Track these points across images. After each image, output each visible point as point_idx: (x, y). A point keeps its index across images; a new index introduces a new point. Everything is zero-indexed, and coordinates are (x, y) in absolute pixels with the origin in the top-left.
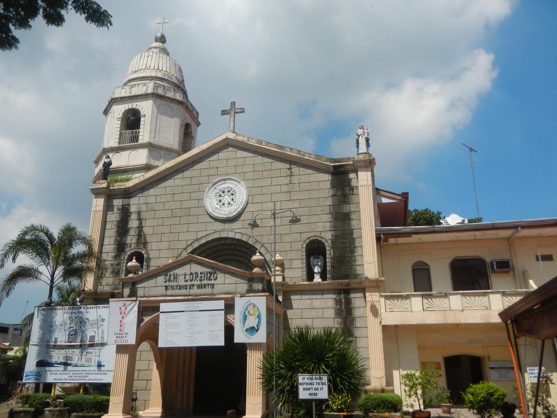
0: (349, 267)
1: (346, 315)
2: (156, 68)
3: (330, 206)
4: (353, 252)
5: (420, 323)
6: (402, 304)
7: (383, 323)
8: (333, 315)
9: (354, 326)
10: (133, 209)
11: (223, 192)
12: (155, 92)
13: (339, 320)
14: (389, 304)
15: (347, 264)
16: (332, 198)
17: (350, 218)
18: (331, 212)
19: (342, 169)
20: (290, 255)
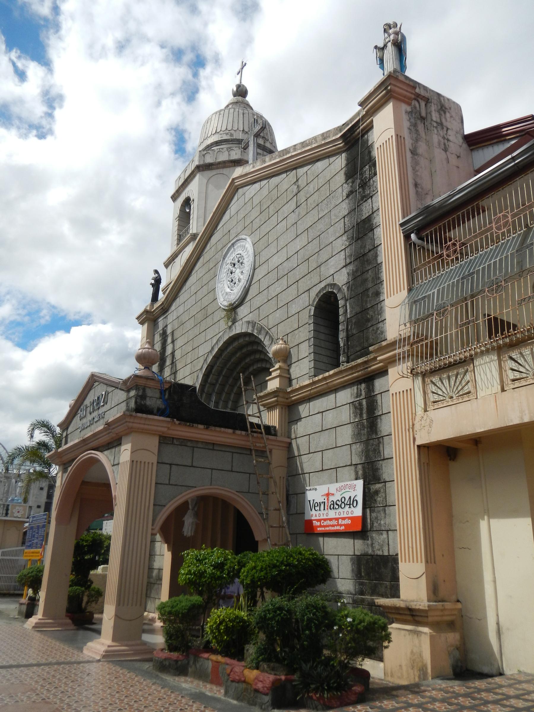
0: (373, 330)
1: (369, 434)
3: (344, 217)
4: (378, 294)
5: (492, 428)
6: (452, 383)
7: (419, 442)
8: (350, 436)
9: (380, 455)
10: (169, 331)
11: (234, 265)
12: (202, 163)
13: (358, 448)
14: (433, 393)
15: (370, 325)
16: (347, 201)
17: (373, 224)
18: (346, 230)
19: (356, 133)
20: (297, 336)
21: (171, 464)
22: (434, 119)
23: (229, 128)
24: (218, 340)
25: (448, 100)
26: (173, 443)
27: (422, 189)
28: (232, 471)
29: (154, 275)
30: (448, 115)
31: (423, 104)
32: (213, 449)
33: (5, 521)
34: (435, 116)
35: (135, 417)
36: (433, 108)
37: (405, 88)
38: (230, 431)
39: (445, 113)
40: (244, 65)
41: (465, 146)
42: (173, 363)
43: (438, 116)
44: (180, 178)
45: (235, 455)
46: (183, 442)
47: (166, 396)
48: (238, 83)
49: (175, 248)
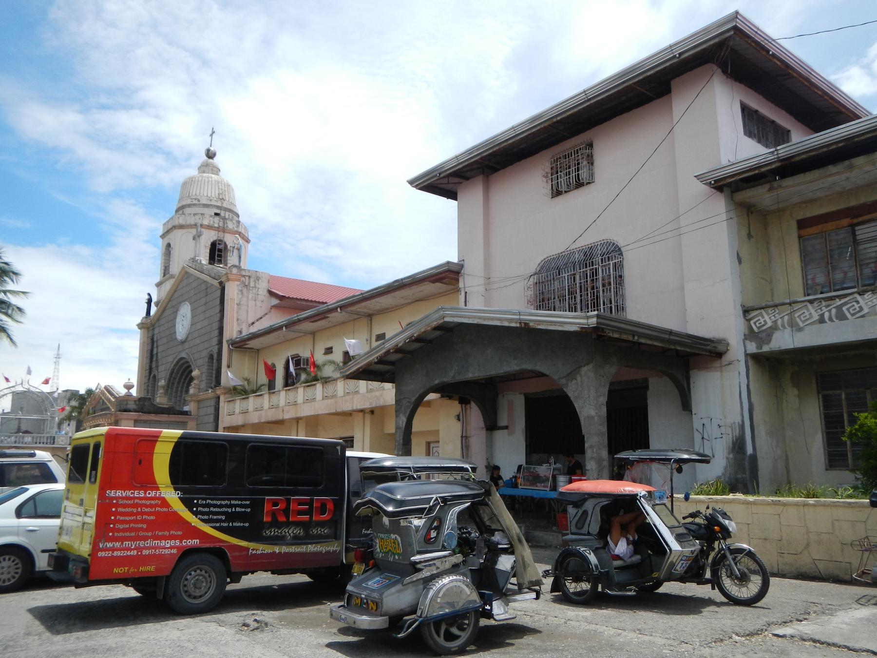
2: (187, 195)
10: (155, 339)
22: (251, 286)
23: (198, 193)
24: (176, 356)
29: (147, 297)
30: (260, 281)
31: (247, 278)
33: (54, 448)
34: (252, 284)
36: (252, 280)
38: (167, 415)
39: (258, 280)
40: (213, 132)
42: (157, 360)
43: (254, 283)
48: (208, 146)
49: (162, 279)
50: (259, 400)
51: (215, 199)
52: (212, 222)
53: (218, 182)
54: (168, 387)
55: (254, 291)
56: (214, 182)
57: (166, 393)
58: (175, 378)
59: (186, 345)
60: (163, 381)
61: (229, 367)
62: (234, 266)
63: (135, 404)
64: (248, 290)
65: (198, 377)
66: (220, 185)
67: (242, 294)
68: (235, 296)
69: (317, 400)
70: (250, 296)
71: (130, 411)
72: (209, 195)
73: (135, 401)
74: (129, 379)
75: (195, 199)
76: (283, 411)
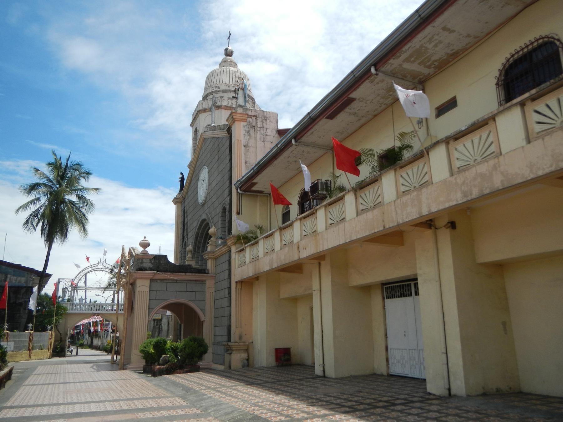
10: (186, 210)
21: (156, 291)
22: (259, 126)
23: (218, 82)
25: (269, 112)
26: (157, 282)
27: (250, 163)
28: (186, 291)
29: (181, 176)
30: (268, 121)
31: (254, 118)
32: (177, 282)
34: (259, 124)
35: (137, 273)
36: (259, 120)
37: (242, 116)
38: (183, 274)
39: (266, 120)
41: (277, 135)
42: (187, 229)
43: (261, 123)
44: (193, 114)
45: (187, 284)
46: (162, 281)
47: (153, 262)
50: (269, 241)
51: (233, 85)
52: (230, 104)
53: (235, 72)
54: (195, 251)
55: (262, 132)
56: (231, 72)
57: (193, 257)
58: (200, 242)
59: (206, 207)
60: (190, 246)
61: (238, 213)
62: (240, 106)
63: (151, 262)
64: (256, 131)
65: (215, 234)
66: (237, 74)
67: (250, 135)
68: (242, 138)
69: (347, 219)
70: (258, 137)
71: (145, 269)
72: (228, 83)
73: (151, 260)
74: (145, 237)
75: (216, 87)
76: (298, 248)
